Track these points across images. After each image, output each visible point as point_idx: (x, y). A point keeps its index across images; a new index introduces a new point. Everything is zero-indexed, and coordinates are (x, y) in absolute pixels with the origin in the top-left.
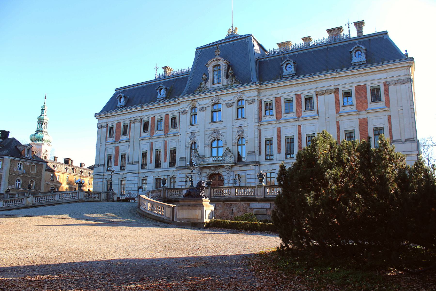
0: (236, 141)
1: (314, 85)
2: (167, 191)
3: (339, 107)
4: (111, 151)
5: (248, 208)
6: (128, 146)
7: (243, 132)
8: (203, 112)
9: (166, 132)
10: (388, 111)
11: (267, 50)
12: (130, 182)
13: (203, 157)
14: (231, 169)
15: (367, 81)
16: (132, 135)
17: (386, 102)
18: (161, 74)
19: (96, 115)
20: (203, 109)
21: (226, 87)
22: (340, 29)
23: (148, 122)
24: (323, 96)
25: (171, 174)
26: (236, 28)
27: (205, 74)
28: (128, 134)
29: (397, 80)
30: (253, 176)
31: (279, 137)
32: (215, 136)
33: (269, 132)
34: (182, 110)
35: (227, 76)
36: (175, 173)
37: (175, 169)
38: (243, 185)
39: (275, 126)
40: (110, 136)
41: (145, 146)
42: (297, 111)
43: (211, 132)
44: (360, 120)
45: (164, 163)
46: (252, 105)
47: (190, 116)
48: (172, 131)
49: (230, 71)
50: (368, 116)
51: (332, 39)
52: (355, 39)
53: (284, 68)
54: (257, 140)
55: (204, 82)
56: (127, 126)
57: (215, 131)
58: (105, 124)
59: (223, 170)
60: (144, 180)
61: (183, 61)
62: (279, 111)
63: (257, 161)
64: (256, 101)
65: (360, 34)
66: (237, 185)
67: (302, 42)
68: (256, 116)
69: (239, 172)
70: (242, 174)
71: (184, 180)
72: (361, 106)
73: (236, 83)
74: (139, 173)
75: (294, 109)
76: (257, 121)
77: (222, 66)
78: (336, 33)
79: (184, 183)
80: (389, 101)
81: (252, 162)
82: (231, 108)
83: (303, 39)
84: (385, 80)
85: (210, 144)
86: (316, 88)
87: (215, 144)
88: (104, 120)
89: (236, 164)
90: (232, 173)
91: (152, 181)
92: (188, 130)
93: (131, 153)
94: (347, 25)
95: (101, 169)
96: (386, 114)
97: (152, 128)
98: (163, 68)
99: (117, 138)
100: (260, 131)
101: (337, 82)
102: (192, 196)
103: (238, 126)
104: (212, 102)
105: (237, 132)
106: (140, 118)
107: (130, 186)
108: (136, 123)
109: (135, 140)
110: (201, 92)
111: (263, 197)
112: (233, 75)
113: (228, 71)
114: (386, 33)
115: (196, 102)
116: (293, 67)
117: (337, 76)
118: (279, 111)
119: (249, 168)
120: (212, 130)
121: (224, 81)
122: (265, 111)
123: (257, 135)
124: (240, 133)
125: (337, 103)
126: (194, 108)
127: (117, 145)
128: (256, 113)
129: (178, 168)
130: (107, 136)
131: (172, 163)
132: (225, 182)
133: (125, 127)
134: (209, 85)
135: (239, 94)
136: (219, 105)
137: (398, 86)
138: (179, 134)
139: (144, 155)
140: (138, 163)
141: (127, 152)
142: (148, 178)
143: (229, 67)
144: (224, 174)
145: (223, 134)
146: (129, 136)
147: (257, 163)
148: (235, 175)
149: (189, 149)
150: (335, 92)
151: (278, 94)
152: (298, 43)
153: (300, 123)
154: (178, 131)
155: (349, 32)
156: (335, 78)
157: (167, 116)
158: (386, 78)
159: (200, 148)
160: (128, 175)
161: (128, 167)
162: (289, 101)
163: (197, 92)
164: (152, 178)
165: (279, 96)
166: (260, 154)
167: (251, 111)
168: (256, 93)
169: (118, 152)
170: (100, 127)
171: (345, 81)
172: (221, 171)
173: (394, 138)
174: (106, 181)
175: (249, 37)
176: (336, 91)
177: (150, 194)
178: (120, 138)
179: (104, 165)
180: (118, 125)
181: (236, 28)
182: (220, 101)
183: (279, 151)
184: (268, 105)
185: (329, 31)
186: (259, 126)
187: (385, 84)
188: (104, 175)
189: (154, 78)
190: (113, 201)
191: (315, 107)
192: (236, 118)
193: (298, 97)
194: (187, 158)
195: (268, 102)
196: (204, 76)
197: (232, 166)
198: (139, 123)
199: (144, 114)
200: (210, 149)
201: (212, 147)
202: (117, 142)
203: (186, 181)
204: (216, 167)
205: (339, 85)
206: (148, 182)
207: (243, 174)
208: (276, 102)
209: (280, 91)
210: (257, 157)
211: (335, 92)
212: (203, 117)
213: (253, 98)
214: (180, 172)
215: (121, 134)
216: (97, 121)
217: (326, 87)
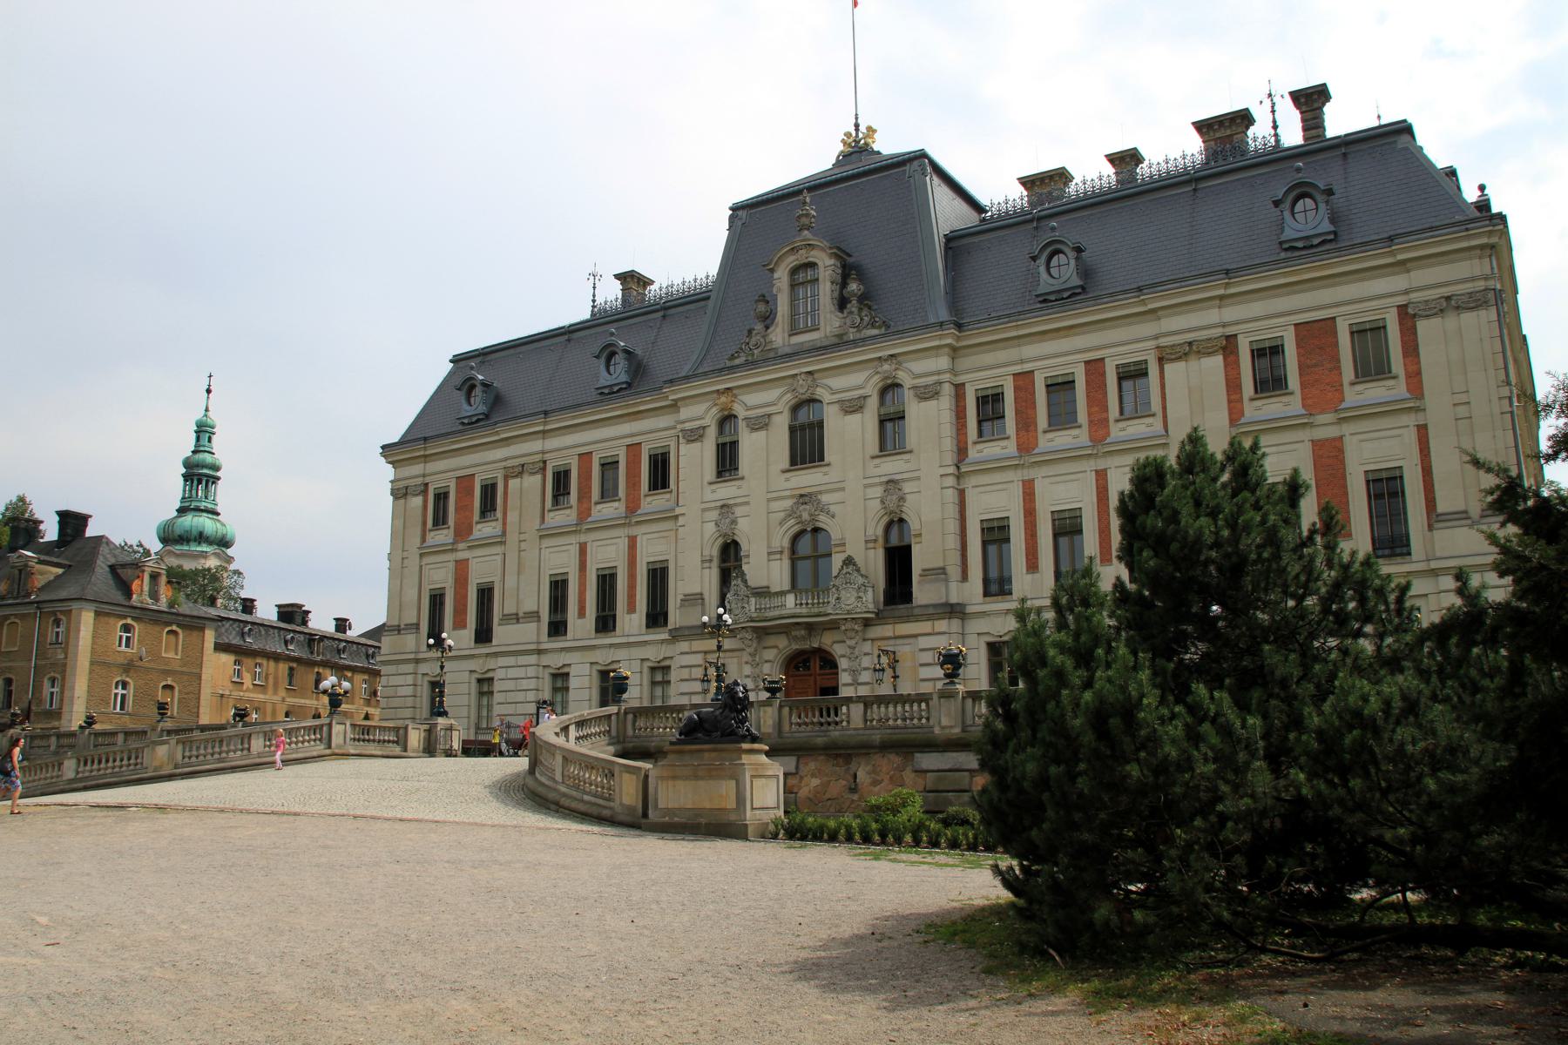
0: (880, 531)
1: (1147, 329)
2: (630, 717)
3: (1241, 400)
4: (441, 575)
5: (909, 769)
6: (499, 558)
7: (902, 499)
8: (763, 433)
9: (632, 507)
10: (1417, 410)
11: (984, 200)
12: (510, 685)
13: (762, 593)
14: (864, 631)
15: (1337, 305)
16: (512, 517)
17: (1408, 376)
18: (611, 297)
19: (385, 448)
20: (760, 424)
21: (840, 343)
22: (1243, 118)
23: (567, 473)
24: (1181, 365)
25: (654, 654)
26: (869, 129)
27: (763, 299)
28: (499, 514)
29: (1448, 298)
32: (806, 516)
33: (995, 499)
34: (688, 426)
35: (842, 303)
36: (666, 651)
37: (665, 636)
38: (905, 688)
39: (1016, 476)
40: (436, 523)
41: (561, 559)
42: (1091, 422)
43: (788, 503)
44: (1317, 445)
45: (627, 617)
46: (933, 403)
47: (714, 448)
48: (654, 503)
49: (853, 286)
50: (1346, 429)
51: (1212, 154)
52: (1295, 154)
53: (1042, 269)
54: (953, 526)
55: (759, 327)
56: (494, 486)
57: (804, 498)
58: (419, 481)
59: (836, 636)
60: (560, 678)
61: (687, 252)
62: (1026, 423)
63: (953, 600)
64: (947, 389)
65: (1314, 132)
66: (885, 690)
67: (1109, 170)
68: (949, 444)
69: (892, 642)
70: (904, 650)
71: (699, 673)
72: (1323, 392)
73: (873, 327)
74: (539, 652)
76: (950, 458)
77: (821, 269)
78: (1228, 132)
79: (698, 686)
80: (1419, 373)
81: (935, 606)
82: (857, 417)
83: (1114, 159)
84: (1401, 300)
85: (786, 543)
86: (1156, 337)
87: (805, 546)
88: (417, 469)
89: (879, 618)
90: (867, 647)
91: (586, 682)
92: (709, 496)
93: (511, 582)
94: (1267, 103)
95: (409, 641)
96: (1411, 420)
97: (584, 494)
98: (617, 277)
99: (463, 532)
100: (962, 493)
101: (1231, 313)
102: (708, 733)
103: (884, 479)
104: (789, 396)
105: (882, 502)
106: (538, 457)
107: (511, 697)
108: (525, 476)
109: (523, 537)
110: (751, 364)
111: (957, 730)
112: (864, 299)
113: (844, 285)
114: (1403, 129)
115: (735, 396)
116: (1073, 262)
118: (1026, 423)
119: (925, 626)
121: (830, 322)
122: (980, 422)
123: (952, 511)
124: (892, 506)
125: (1233, 385)
126: (727, 419)
127: (461, 555)
128: (948, 430)
129: (677, 635)
130: (424, 523)
131: (657, 617)
132: (844, 678)
133: (489, 491)
134: (778, 336)
135: (886, 367)
136: (817, 405)
137: (1451, 321)
138: (678, 511)
139: (558, 588)
140: (534, 616)
141: (497, 580)
142: (573, 671)
143: (848, 270)
144: (838, 650)
145: (832, 508)
146: (504, 524)
147: (954, 611)
148: (876, 652)
149: (715, 563)
150: (1224, 349)
151: (1022, 362)
152: (1091, 175)
153: (1101, 464)
154: (672, 503)
155: (1275, 127)
156: (1221, 298)
157: (633, 449)
158: (1406, 292)
159: (751, 560)
160: (502, 661)
161: (503, 634)
162: (1060, 387)
163: (737, 362)
164: (586, 669)
165: (1027, 367)
166: (965, 577)
167: (928, 421)
168: (943, 362)
169: (466, 580)
170: (400, 493)
171: (1257, 308)
173: (1441, 507)
174: (426, 685)
175: (916, 163)
176: (1228, 346)
177: (572, 728)
178: (470, 532)
179: (417, 626)
180: (465, 482)
181: (869, 129)
182: (821, 393)
184: (990, 405)
185: (1202, 127)
186: (959, 477)
187: (1402, 309)
188: (417, 661)
189: (587, 316)
190: (449, 753)
191: (1156, 405)
192: (877, 452)
193: (1095, 368)
194: (706, 596)
195: (990, 392)
196: (761, 307)
197: (867, 623)
198: (539, 477)
199: (553, 443)
200: (786, 563)
201: (794, 559)
202: (461, 546)
203: (705, 680)
204: (811, 628)
205: (1237, 323)
206: (573, 683)
207: (907, 649)
208: (1016, 389)
209: (1030, 350)
210: (953, 586)
211: (1224, 349)
212: (764, 451)
214: (684, 646)
215: (476, 517)
216: (389, 472)
217: (1190, 330)
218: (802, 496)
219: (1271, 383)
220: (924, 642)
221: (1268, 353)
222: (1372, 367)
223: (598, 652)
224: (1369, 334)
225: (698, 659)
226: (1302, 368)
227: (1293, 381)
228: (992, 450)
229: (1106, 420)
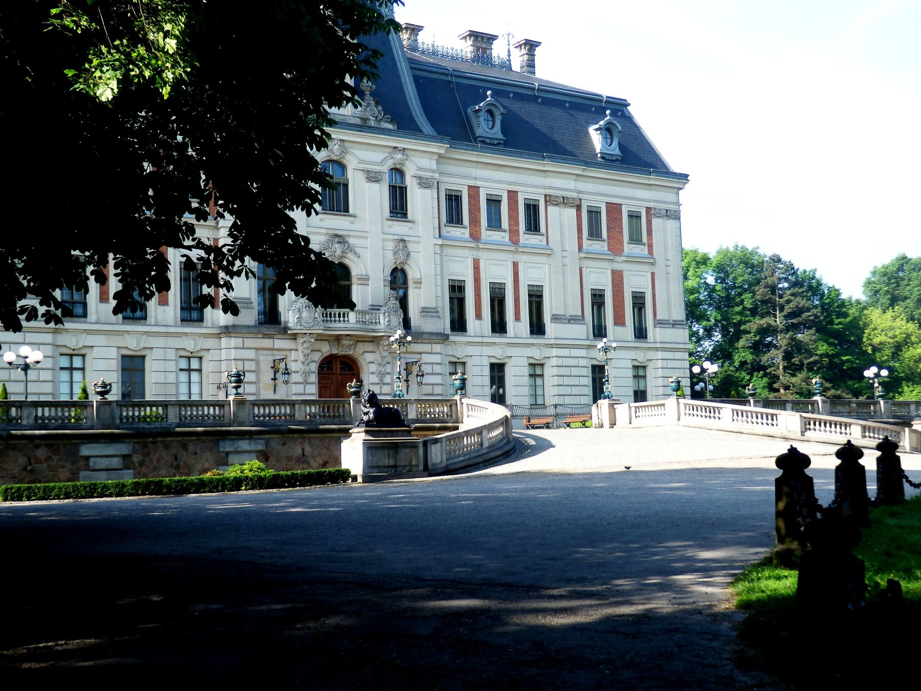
1: (539, 180)
7: (408, 255)
15: (625, 198)
22: (491, 38)
30: (438, 369)
31: (477, 280)
32: (338, 252)
59: (369, 347)
62: (474, 221)
75: (505, 224)
96: (648, 269)
101: (582, 186)
117: (585, 174)
118: (474, 221)
120: (326, 234)
135: (399, 156)
145: (357, 250)
155: (509, 56)
156: (577, 175)
162: (494, 202)
164: (114, 353)
165: (478, 184)
168: (433, 164)
172: (361, 348)
183: (479, 316)
187: (648, 209)
193: (512, 195)
213: (430, 174)
218: (337, 236)
219: (595, 233)
220: (426, 358)
221: (594, 214)
222: (635, 239)
223: (127, 337)
224: (634, 217)
225: (251, 354)
226: (608, 227)
227: (605, 235)
228: (455, 232)
229: (518, 231)
